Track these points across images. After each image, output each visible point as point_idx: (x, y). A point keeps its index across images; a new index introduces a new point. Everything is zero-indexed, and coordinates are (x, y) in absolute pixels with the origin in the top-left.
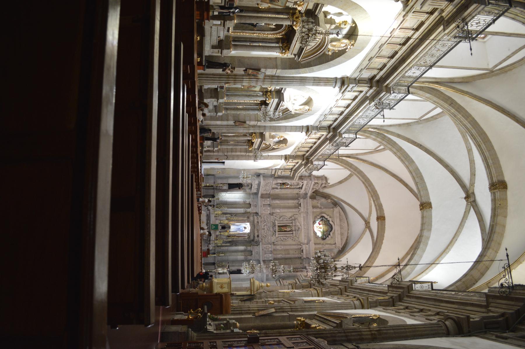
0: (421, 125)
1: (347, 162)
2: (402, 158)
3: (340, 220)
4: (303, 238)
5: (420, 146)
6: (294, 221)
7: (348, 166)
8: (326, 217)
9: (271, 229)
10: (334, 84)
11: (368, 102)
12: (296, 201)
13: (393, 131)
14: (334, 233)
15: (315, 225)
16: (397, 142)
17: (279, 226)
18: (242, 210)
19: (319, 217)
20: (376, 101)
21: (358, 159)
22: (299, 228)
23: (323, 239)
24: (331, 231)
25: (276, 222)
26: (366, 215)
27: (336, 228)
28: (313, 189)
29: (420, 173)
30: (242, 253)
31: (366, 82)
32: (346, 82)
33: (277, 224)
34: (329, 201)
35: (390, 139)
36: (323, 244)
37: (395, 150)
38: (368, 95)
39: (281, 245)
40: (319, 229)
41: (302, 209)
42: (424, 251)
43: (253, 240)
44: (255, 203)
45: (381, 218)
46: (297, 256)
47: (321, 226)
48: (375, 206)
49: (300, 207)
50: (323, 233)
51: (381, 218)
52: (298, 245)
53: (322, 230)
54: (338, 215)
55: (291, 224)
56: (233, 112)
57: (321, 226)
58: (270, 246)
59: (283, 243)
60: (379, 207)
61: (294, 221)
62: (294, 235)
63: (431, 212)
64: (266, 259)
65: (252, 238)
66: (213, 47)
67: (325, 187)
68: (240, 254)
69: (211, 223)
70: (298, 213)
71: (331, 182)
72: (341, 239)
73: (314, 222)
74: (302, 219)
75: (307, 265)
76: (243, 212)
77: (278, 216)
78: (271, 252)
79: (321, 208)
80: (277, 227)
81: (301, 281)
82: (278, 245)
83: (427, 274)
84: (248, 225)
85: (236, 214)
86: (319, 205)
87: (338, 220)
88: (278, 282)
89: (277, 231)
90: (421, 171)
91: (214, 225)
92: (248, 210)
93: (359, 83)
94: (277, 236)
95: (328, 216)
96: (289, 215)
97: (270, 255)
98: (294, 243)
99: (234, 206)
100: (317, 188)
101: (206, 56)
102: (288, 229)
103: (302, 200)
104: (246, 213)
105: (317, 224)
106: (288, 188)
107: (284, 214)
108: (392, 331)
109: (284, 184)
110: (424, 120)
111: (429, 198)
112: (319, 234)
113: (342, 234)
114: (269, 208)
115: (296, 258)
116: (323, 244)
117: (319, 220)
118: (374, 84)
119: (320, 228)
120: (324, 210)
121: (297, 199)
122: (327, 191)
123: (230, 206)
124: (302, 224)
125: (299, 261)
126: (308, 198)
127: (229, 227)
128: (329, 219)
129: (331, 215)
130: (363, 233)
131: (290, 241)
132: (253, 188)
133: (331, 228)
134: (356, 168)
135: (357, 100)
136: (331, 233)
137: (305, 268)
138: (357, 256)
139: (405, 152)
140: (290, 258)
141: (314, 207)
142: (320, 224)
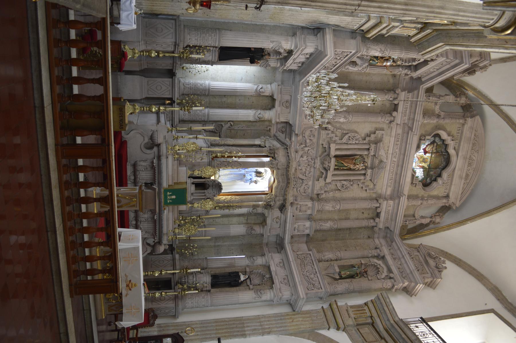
6: (373, 146)
9: (318, 164)
12: (389, 97)
17: (336, 156)
18: (247, 114)
22: (381, 161)
23: (426, 184)
24: (444, 168)
25: (333, 147)
27: (458, 163)
30: (242, 219)
33: (333, 153)
36: (422, 198)
39: (336, 200)
41: (399, 117)
44: (287, 97)
50: (427, 171)
52: (371, 199)
55: (366, 153)
59: (338, 195)
61: (373, 146)
62: (368, 178)
64: (296, 233)
69: (165, 185)
70: (385, 126)
74: (393, 140)
76: (251, 119)
77: (339, 133)
78: (310, 218)
79: (439, 116)
80: (333, 160)
84: (268, 174)
86: (437, 109)
91: (174, 191)
92: (267, 115)
94: (328, 180)
95: (449, 135)
97: (308, 224)
98: (364, 194)
99: (230, 100)
103: (403, 95)
104: (261, 121)
107: (354, 127)
112: (420, 173)
115: (360, 228)
116: (422, 198)
119: (424, 161)
120: (441, 122)
121: (392, 89)
123: (217, 100)
124: (390, 151)
129: (454, 132)
131: (356, 192)
132: (290, 61)
133: (448, 161)
141: (427, 113)
142: (425, 152)
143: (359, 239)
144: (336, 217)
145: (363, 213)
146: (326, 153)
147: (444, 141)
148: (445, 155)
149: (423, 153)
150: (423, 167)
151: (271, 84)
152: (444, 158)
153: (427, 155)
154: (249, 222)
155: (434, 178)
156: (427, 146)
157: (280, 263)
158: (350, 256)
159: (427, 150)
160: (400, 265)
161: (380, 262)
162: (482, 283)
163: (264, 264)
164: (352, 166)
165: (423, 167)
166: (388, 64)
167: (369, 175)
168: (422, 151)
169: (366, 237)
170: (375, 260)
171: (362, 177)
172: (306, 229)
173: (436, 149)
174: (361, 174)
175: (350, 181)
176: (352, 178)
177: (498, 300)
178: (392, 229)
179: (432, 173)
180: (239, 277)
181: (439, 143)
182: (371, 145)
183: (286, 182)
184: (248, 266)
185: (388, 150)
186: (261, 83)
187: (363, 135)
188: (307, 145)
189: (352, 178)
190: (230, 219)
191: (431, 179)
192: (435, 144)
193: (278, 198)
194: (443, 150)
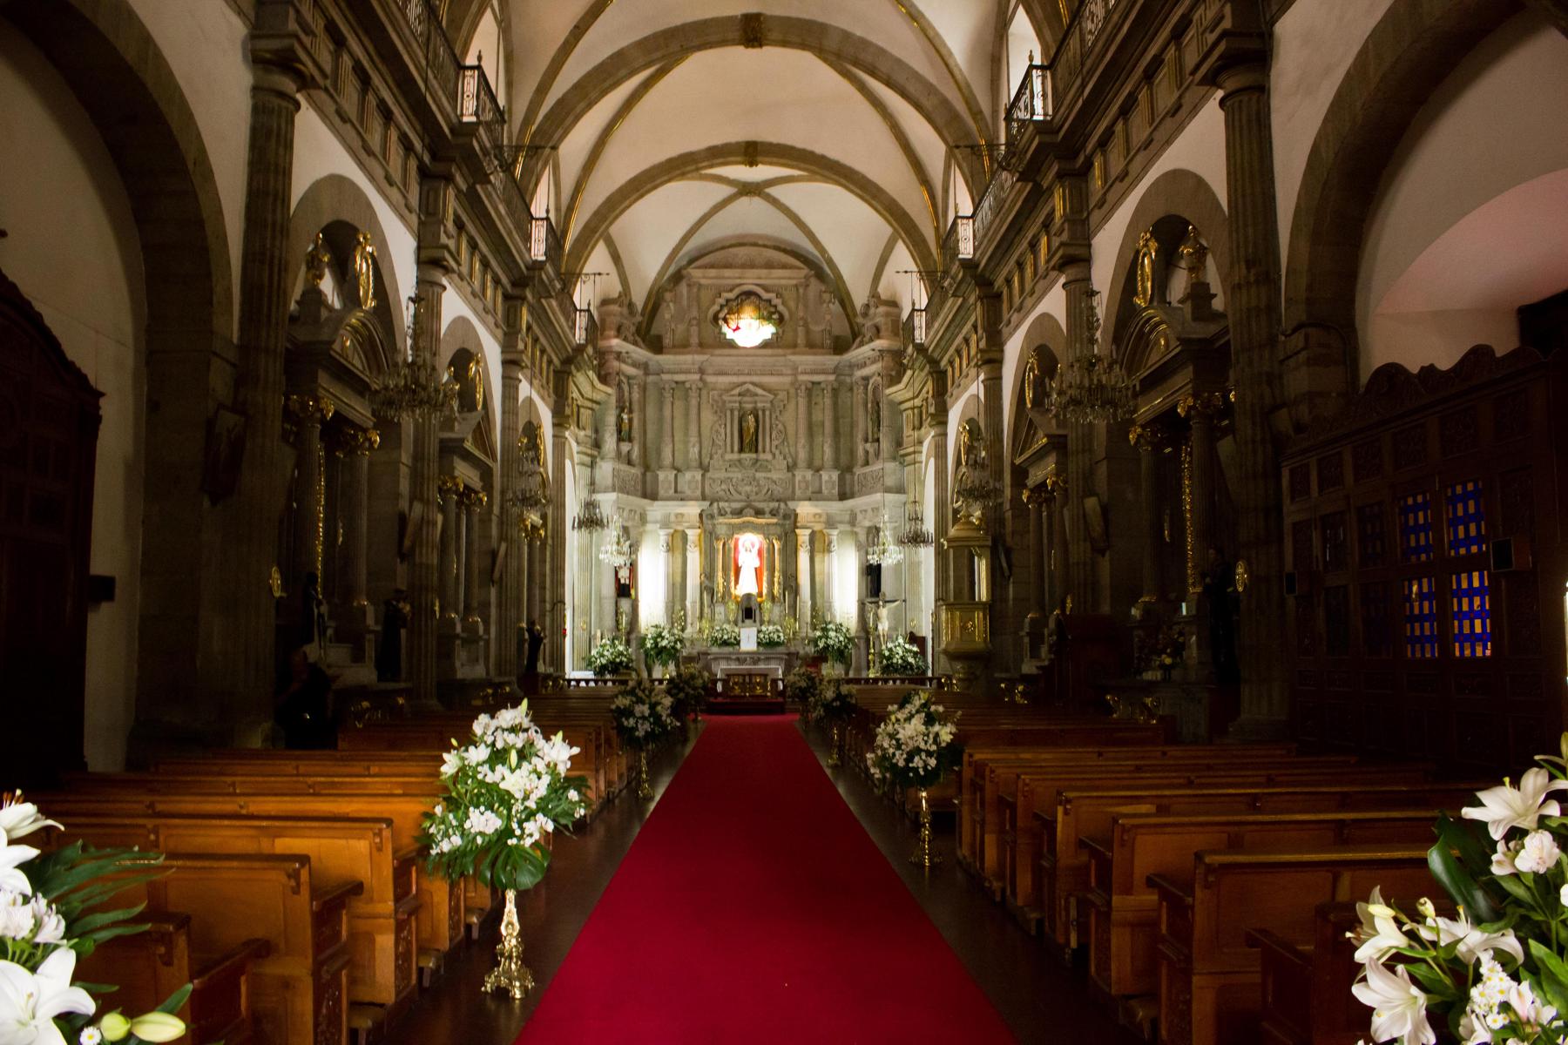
0: (514, 21)
1: (577, 240)
2: (607, 84)
3: (728, 266)
5: (579, 31)
6: (729, 405)
7: (589, 238)
8: (716, 307)
10: (436, 289)
11: (478, 187)
13: (526, 104)
14: (766, 289)
16: (560, 95)
17: (741, 450)
20: (491, 164)
21: (571, 209)
24: (759, 296)
25: (729, 456)
26: (727, 191)
27: (751, 280)
28: (635, 343)
29: (655, 36)
30: (817, 559)
31: (432, 194)
32: (436, 253)
34: (668, 296)
35: (546, 117)
37: (582, 105)
38: (464, 187)
40: (750, 331)
42: (882, 51)
43: (782, 525)
45: (752, 152)
46: (828, 401)
47: (742, 323)
48: (711, 166)
51: (752, 152)
53: (756, 323)
54: (713, 272)
56: (476, 590)
57: (742, 323)
58: (798, 478)
60: (720, 154)
63: (772, 17)
64: (835, 492)
66: (358, 658)
67: (631, 305)
71: (615, 289)
72: (784, 266)
73: (731, 345)
75: (860, 373)
80: (743, 455)
81: (910, 395)
83: (951, 54)
85: (708, 574)
87: (727, 272)
88: (908, 459)
90: (648, 32)
93: (435, 214)
96: (708, 417)
99: (678, 579)
100: (633, 329)
101: (380, 679)
102: (751, 418)
106: (631, 420)
108: (1250, 230)
109: (619, 431)
110: (501, 10)
111: (730, 19)
113: (769, 265)
114: (688, 475)
115: (835, 405)
118: (440, 168)
122: (639, 297)
124: (735, 379)
125: (844, 396)
127: (748, 596)
128: (721, 301)
130: (775, 202)
133: (749, 294)
134: (596, 214)
135: (465, 218)
136: (765, 296)
137: (866, 379)
138: (844, 229)
139: (589, 75)
140: (836, 420)
158: (862, 423)
166: (625, 416)
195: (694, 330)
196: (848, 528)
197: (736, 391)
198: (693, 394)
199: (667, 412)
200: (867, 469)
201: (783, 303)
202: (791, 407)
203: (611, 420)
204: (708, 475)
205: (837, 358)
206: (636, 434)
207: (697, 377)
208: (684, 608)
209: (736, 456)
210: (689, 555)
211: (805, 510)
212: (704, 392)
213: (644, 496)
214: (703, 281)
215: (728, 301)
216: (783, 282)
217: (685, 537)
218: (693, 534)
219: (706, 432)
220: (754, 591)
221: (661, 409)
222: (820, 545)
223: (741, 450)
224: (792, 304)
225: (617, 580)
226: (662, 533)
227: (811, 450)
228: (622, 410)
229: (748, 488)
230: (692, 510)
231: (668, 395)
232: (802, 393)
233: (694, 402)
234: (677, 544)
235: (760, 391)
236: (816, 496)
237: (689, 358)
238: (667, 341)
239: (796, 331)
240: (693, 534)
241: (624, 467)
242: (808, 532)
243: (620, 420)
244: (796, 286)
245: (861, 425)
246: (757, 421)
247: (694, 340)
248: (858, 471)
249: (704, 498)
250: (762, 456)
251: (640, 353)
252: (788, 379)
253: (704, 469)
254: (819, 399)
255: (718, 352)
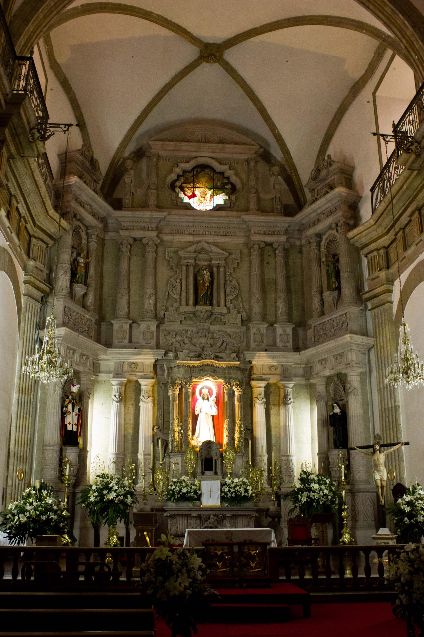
4: (235, 241)
6: (184, 261)
8: (173, 176)
15: (195, 207)
17: (196, 303)
19: (174, 195)
25: (184, 309)
27: (205, 155)
30: (273, 412)
33: (191, 309)
40: (204, 200)
46: (280, 260)
47: (197, 192)
49: (145, 241)
53: (209, 193)
54: (171, 145)
55: (191, 269)
57: (197, 192)
58: (253, 331)
64: (290, 344)
65: (239, 375)
68: (273, 419)
73: (188, 207)
74: (177, 238)
80: (198, 307)
81: (380, 231)
82: (251, 310)
85: (162, 425)
87: (185, 146)
89: (209, 308)
95: (171, 171)
96: (164, 272)
97: (279, 330)
99: (130, 431)
102: (206, 273)
105: (195, 203)
109: (74, 274)
112: (220, 199)
113: (223, 141)
114: (143, 326)
115: (287, 264)
117: (181, 195)
119: (204, 195)
124: (190, 238)
126: (118, 213)
127: (208, 444)
128: (178, 171)
130: (231, 71)
133: (203, 167)
136: (219, 168)
137: (319, 236)
140: (288, 278)
142: (194, 196)
143: (302, 265)
144: (273, 296)
145: (268, 263)
146: (192, 316)
147: (179, 176)
148: (197, 171)
149: (195, 198)
150: (212, 196)
151: (112, 385)
152: (201, 172)
153: (196, 193)
154: (277, 403)
155: (226, 181)
156: (186, 195)
157: (322, 364)
158: (317, 276)
159: (190, 194)
160: (324, 214)
161: (324, 237)
162: (348, 106)
163: (324, 383)
164: (208, 284)
165: (212, 196)
167: (218, 262)
168: (192, 199)
169: (299, 256)
170: (322, 244)
171: (222, 269)
172: (286, 331)
173: (190, 183)
174: (218, 272)
175: (225, 284)
176: (222, 282)
177: (364, 86)
178: (287, 225)
179: (219, 184)
180: (335, 414)
181: (183, 181)
182: (181, 263)
183: (208, 367)
184: (327, 403)
185: (189, 242)
186: (110, 397)
187: (171, 274)
188: (181, 339)
189: (222, 282)
190: (273, 425)
191: (227, 184)
192: (184, 185)
193: (227, 376)
194: (191, 175)
195: (153, 192)
196: (303, 382)
197: (192, 248)
198: (150, 250)
199: (124, 265)
200: (326, 319)
201: (236, 174)
202: (244, 266)
203: (66, 258)
204: (163, 327)
205: (289, 219)
206: (92, 280)
207: (154, 234)
208: (135, 461)
209: (191, 309)
210: (142, 406)
211: (261, 361)
212: (160, 249)
213: (98, 341)
214: (162, 153)
215: (184, 172)
216: (235, 156)
217: (138, 387)
218: (146, 384)
219: (161, 285)
220: (212, 438)
221: (118, 264)
222: (276, 399)
223: (196, 303)
224: (244, 176)
225: (63, 426)
226: (114, 382)
227: (264, 306)
228: (79, 255)
229: (203, 340)
230: (147, 359)
231: (125, 250)
232: (255, 252)
233: (150, 257)
234: (129, 396)
235: (215, 249)
236: (271, 347)
237: (147, 214)
238: (127, 201)
239: (248, 199)
240: (146, 384)
241: (76, 308)
242: (263, 384)
243: (74, 264)
244: (248, 161)
245: (315, 279)
246: (212, 276)
247: (153, 201)
248: (314, 322)
249: (158, 347)
250: (217, 310)
251: (101, 204)
252: (240, 241)
253: (160, 321)
254: (271, 259)
255: (174, 212)
